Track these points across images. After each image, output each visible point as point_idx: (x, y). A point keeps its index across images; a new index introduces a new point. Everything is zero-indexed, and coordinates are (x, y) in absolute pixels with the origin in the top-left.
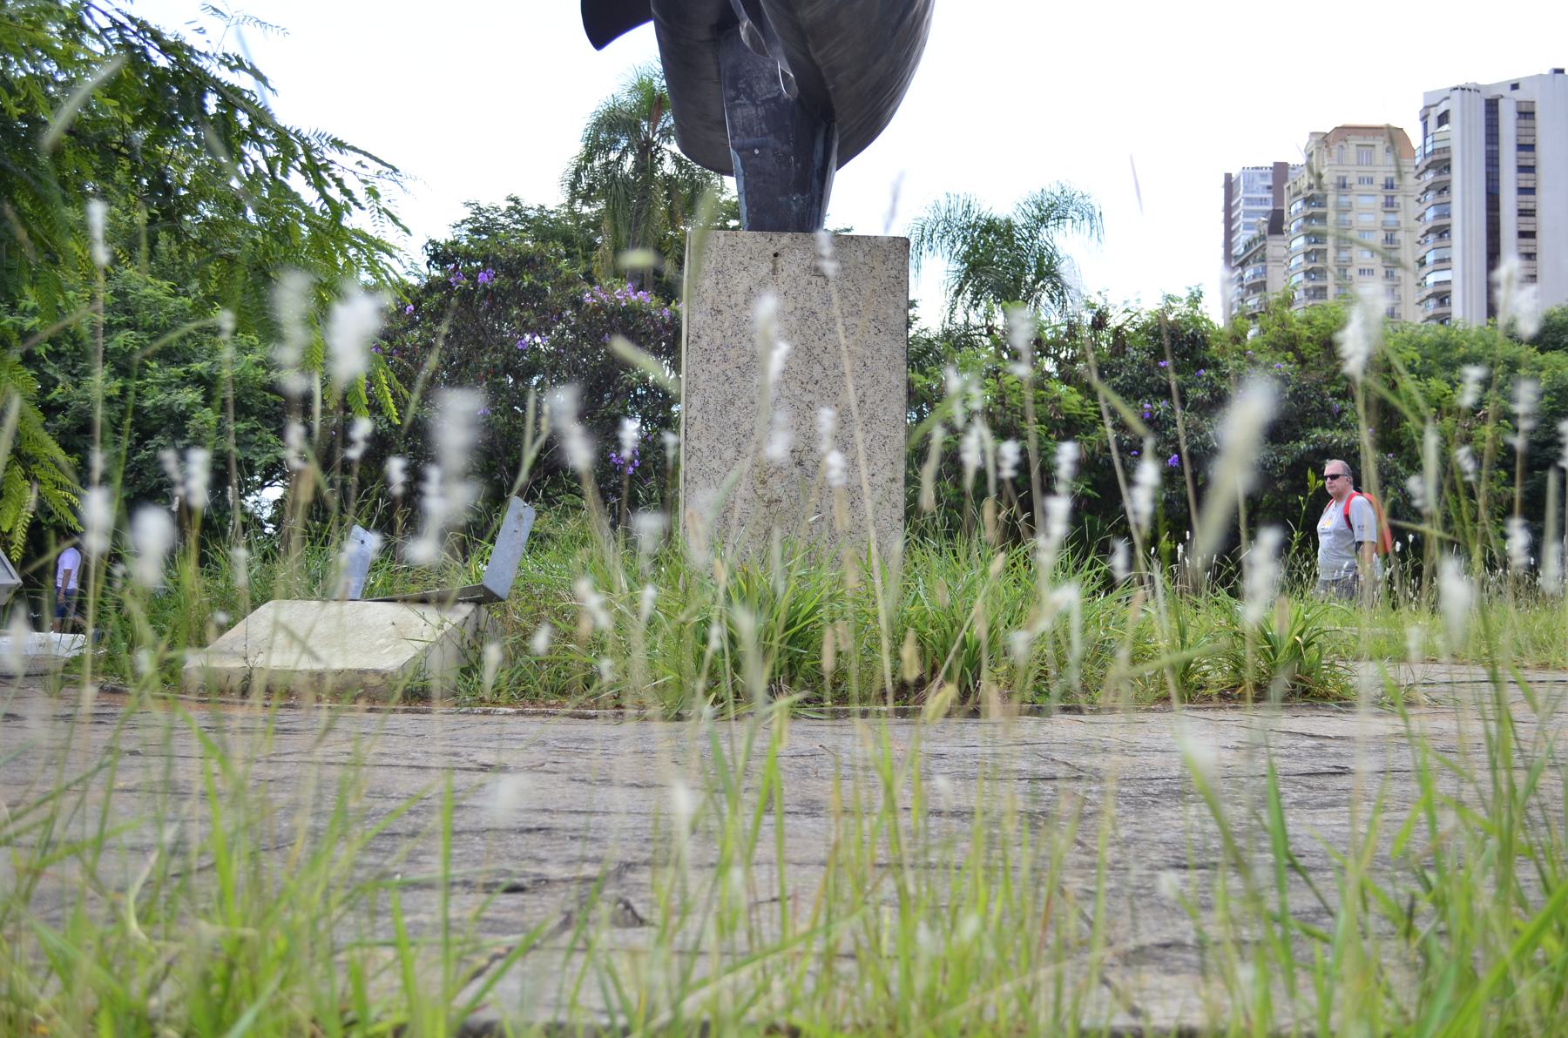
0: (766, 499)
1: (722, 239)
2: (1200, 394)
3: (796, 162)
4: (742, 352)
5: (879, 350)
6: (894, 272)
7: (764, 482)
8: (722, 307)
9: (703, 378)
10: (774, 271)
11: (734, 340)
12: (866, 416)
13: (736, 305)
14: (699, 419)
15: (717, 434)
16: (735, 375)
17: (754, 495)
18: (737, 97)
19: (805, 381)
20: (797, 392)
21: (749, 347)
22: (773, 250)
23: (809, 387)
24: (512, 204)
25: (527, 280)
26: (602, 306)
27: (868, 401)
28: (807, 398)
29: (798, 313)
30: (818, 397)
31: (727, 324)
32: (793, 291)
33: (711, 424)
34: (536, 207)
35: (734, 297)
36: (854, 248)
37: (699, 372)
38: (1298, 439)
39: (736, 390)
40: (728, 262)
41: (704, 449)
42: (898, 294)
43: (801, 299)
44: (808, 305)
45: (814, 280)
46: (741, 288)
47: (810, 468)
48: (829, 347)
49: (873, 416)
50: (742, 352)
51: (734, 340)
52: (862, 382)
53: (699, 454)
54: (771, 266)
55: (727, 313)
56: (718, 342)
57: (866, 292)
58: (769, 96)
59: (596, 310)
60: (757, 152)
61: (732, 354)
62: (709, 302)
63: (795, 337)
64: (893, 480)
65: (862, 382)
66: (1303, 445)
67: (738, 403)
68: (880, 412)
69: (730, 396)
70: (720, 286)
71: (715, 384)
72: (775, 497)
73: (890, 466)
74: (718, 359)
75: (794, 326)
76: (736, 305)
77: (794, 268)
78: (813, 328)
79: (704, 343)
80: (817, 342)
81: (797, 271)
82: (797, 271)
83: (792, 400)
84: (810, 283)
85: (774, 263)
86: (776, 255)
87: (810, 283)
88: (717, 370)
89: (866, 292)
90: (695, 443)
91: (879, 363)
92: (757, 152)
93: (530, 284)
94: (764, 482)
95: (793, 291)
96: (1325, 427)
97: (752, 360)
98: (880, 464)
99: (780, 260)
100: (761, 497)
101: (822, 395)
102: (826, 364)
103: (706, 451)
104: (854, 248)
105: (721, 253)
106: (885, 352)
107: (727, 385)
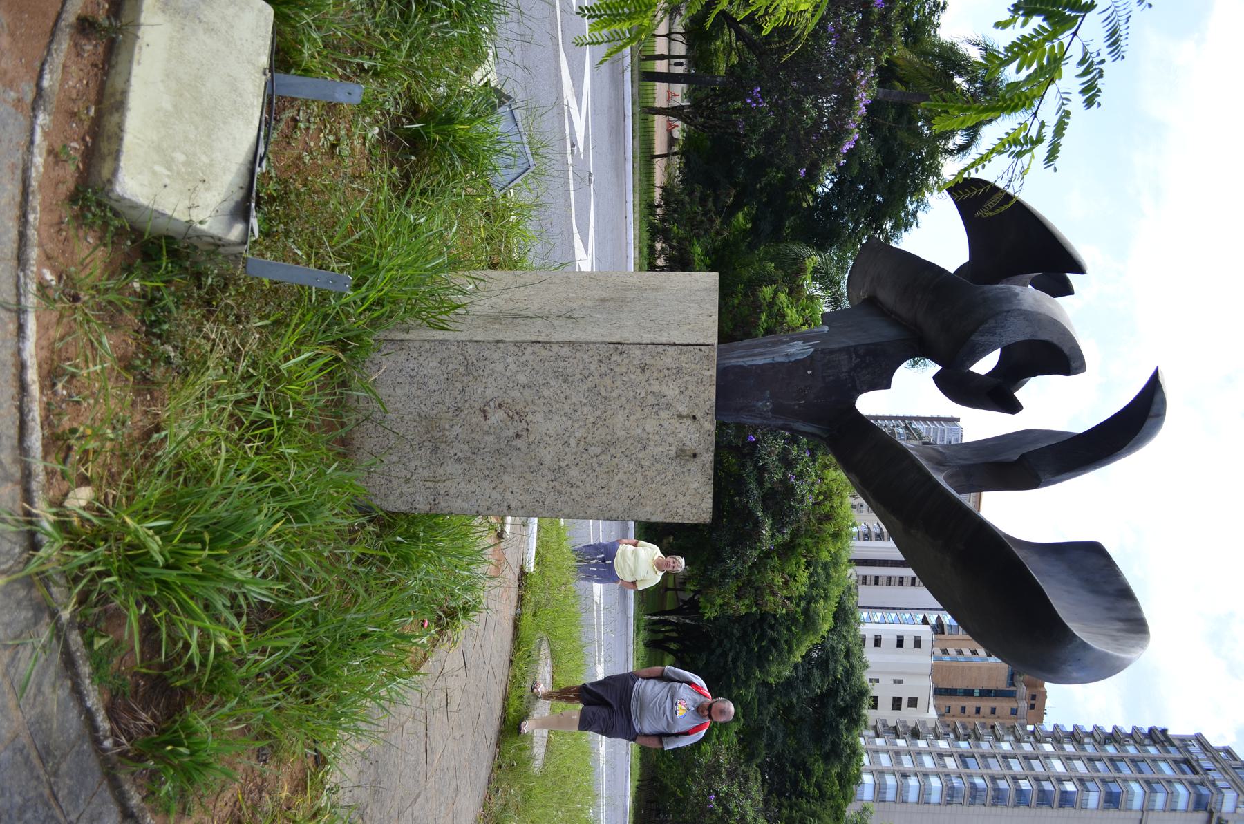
0: (486, 408)
1: (708, 373)
2: (794, 453)
3: (799, 404)
4: (609, 390)
5: (615, 499)
6: (681, 511)
7: (500, 406)
8: (648, 373)
9: (586, 357)
10: (680, 416)
11: (619, 383)
15: (538, 368)
16: (589, 383)
17: (488, 399)
18: (857, 356)
19: (587, 440)
20: (577, 434)
21: (614, 395)
22: (699, 415)
23: (582, 444)
24: (941, 5)
25: (876, 31)
26: (855, 84)
27: (572, 490)
28: (573, 442)
29: (645, 436)
30: (574, 450)
31: (633, 377)
32: (663, 432)
33: (546, 364)
34: (940, 21)
35: (657, 382)
36: (701, 480)
37: (591, 353)
38: (763, 511)
39: (577, 384)
40: (688, 378)
41: (524, 358)
42: (663, 514)
43: (657, 437)
44: (652, 443)
45: (673, 448)
46: (664, 389)
47: (514, 444)
49: (560, 493)
50: (609, 390)
51: (619, 383)
52: (588, 485)
53: (520, 354)
54: (685, 414)
55: (642, 377)
56: (616, 369)
57: (663, 490)
58: (858, 382)
59: (853, 80)
60: (809, 372)
61: (607, 381)
62: (652, 362)
63: (623, 433)
65: (588, 485)
66: (760, 514)
67: (565, 386)
68: (564, 498)
69: (571, 379)
70: (666, 371)
71: (581, 367)
72: (489, 415)
76: (650, 385)
77: (683, 432)
78: (632, 448)
79: (616, 357)
80: (620, 450)
84: (670, 445)
85: (687, 416)
86: (694, 417)
88: (592, 368)
89: (663, 490)
90: (529, 350)
92: (809, 372)
93: (873, 34)
94: (500, 406)
96: (772, 526)
98: (521, 498)
99: (690, 421)
100: (487, 404)
101: (576, 454)
102: (603, 457)
103: (523, 359)
104: (701, 480)
105: (695, 372)
106: (614, 504)
107: (580, 377)
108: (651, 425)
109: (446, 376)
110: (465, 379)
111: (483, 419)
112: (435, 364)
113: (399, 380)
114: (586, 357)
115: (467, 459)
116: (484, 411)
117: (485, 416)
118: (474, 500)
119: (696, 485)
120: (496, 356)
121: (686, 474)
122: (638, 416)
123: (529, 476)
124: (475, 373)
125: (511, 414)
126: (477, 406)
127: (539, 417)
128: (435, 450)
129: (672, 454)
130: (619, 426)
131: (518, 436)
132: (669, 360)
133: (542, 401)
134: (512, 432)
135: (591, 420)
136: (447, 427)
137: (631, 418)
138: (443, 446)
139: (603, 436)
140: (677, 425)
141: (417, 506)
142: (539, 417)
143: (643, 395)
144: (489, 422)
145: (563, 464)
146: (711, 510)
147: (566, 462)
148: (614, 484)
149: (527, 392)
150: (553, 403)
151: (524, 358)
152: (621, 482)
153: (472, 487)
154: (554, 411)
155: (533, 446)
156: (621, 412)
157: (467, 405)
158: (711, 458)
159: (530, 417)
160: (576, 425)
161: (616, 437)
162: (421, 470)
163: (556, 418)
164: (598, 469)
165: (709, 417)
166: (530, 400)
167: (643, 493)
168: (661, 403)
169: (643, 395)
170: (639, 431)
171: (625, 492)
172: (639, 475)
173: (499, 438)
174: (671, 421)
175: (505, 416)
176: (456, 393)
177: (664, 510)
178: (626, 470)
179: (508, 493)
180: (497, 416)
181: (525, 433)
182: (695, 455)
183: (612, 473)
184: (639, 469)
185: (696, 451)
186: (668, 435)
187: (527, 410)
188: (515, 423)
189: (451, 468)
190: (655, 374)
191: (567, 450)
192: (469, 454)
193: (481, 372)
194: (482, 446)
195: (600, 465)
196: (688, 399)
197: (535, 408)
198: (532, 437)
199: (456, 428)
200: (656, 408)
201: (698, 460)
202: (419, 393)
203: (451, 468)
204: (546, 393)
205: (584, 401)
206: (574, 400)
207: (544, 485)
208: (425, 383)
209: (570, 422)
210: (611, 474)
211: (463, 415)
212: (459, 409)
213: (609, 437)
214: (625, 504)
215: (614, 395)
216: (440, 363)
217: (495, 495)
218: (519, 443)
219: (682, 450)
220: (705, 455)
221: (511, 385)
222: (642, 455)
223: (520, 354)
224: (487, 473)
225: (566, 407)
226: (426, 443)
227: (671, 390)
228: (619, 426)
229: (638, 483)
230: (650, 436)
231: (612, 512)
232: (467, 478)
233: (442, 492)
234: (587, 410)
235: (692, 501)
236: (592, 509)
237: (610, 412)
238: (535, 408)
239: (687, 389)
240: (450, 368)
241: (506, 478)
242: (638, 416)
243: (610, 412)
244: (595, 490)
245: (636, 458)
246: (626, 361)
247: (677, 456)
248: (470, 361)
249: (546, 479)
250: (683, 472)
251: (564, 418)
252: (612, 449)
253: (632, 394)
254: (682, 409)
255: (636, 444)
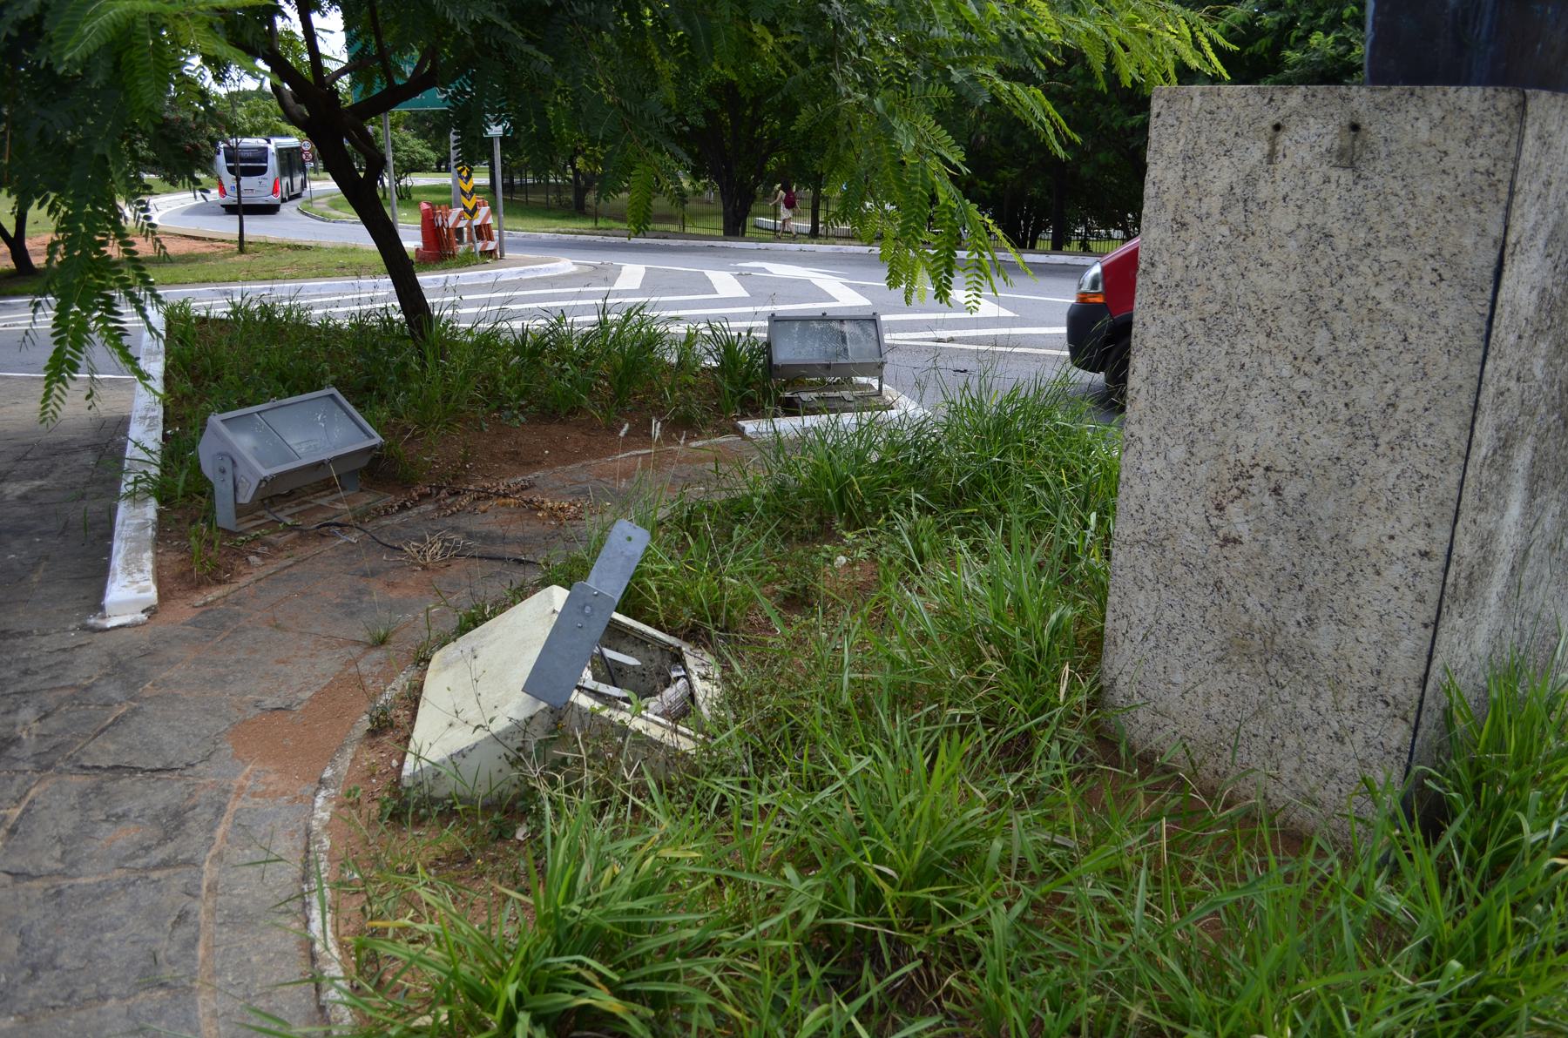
1: (1197, 101)
5: (1434, 314)
6: (1484, 163)
7: (1220, 508)
8: (1188, 218)
9: (1153, 330)
10: (1271, 157)
11: (1200, 274)
12: (1395, 433)
13: (1208, 215)
14: (1143, 392)
15: (1164, 421)
16: (1196, 330)
17: (1205, 524)
19: (1300, 355)
20: (1286, 373)
21: (1220, 287)
22: (1272, 117)
23: (1306, 367)
27: (1402, 407)
28: (1301, 384)
29: (1302, 234)
30: (1318, 385)
31: (1192, 247)
32: (1298, 194)
33: (1159, 404)
35: (1205, 200)
36: (1413, 113)
37: (1148, 320)
39: (1196, 356)
40: (1202, 141)
41: (1146, 440)
42: (1487, 206)
43: (1309, 208)
44: (1320, 220)
45: (1334, 174)
46: (1219, 186)
47: (1291, 503)
48: (1347, 299)
49: (1406, 435)
50: (1210, 294)
51: (1200, 274)
53: (1139, 446)
54: (1267, 148)
55: (1195, 228)
56: (1178, 276)
57: (1426, 202)
61: (1196, 296)
62: (1170, 207)
63: (1293, 277)
64: (1425, 555)
67: (1197, 377)
68: (1420, 429)
69: (1187, 365)
70: (1189, 182)
71: (1168, 342)
72: (1234, 534)
73: (1421, 530)
74: (1176, 302)
75: (1294, 257)
76: (1208, 215)
77: (1304, 151)
78: (1324, 263)
80: (1327, 289)
81: (1308, 158)
82: (1308, 158)
83: (1276, 385)
84: (1327, 180)
85: (1273, 142)
86: (1277, 127)
87: (1327, 180)
88: (1172, 321)
89: (1426, 202)
91: (1432, 339)
94: (1220, 508)
95: (1298, 194)
97: (1223, 308)
98: (1407, 521)
99: (1283, 137)
101: (1325, 383)
102: (1338, 328)
106: (1446, 320)
107: (1184, 345)
108: (1283, 219)
109: (1160, 586)
110: (1169, 555)
111: (1239, 548)
112: (1141, 596)
113: (1160, 669)
114: (1153, 330)
115: (1309, 603)
116: (1226, 540)
117: (1235, 541)
118: (1397, 624)
119: (1423, 125)
120: (1139, 490)
121: (1394, 147)
122: (1262, 244)
123: (1361, 491)
124: (1163, 534)
125: (1235, 492)
126: (1215, 550)
127: (1247, 439)
128: (1286, 659)
129: (1346, 177)
130: (1277, 284)
131: (1277, 491)
132: (1170, 175)
133: (1218, 426)
134: (1270, 502)
135: (1262, 338)
136: (1246, 619)
137: (1266, 257)
138: (1278, 639)
139: (1296, 321)
140: (1287, 163)
141: (1395, 743)
142: (1247, 439)
143: (1224, 230)
144: (1246, 538)
145: (1344, 414)
146: (1490, 91)
147: (1340, 406)
148: (1399, 312)
149: (1203, 451)
150: (1224, 407)
151: (1146, 440)
152: (1397, 296)
153: (1369, 616)
154: (1237, 409)
155: (1300, 466)
156: (1253, 276)
157: (1212, 568)
158: (1364, 91)
159: (1245, 457)
160: (1269, 371)
161: (1298, 294)
162: (1320, 703)
163: (1251, 407)
164: (1362, 342)
165: (1278, 95)
166: (1214, 450)
167: (1429, 250)
168: (1243, 197)
169: (1224, 230)
170: (1292, 244)
171: (1422, 290)
172: (1387, 255)
173: (1277, 529)
174: (1278, 178)
175: (1238, 503)
176: (1190, 581)
177: (1477, 204)
178: (1370, 281)
179: (1392, 546)
180: (1237, 520)
181: (1273, 476)
182: (1355, 127)
183: (1375, 313)
184: (1373, 252)
185: (1345, 122)
186: (1307, 183)
187: (1231, 459)
188: (1254, 489)
189: (1324, 640)
190: (1191, 203)
191: (1315, 399)
192: (1301, 597)
193: (1161, 524)
194: (1288, 566)
195: (1354, 336)
196: (1240, 141)
197: (1229, 442)
198: (1282, 464)
199: (1249, 605)
200: (1252, 206)
201: (1364, 121)
202: (1184, 645)
203: (1324, 640)
204: (1205, 416)
205: (1226, 346)
206: (1222, 366)
207: (1383, 464)
208: (1170, 628)
209: (1262, 382)
210: (1376, 316)
211: (1228, 582)
212: (1218, 584)
213: (1299, 308)
214: (1450, 293)
215: (1220, 287)
216: (1141, 588)
217: (1394, 573)
218: (1291, 490)
219: (1341, 154)
220: (1355, 104)
221: (1186, 475)
222: (1342, 244)
223: (1139, 446)
224: (1342, 576)
225: (1234, 383)
226: (1272, 671)
227: (1222, 175)
228: (1277, 284)
229: (1404, 258)
230: (1304, 222)
231: (1466, 327)
232: (1348, 618)
233: (1371, 681)
234: (1242, 346)
235: (1462, 136)
236: (1453, 371)
237: (1251, 299)
238: (1229, 442)
239: (1222, 142)
240: (1151, 576)
241: (1358, 541)
242: (1262, 244)
243: (1251, 299)
244: (1407, 357)
245: (1348, 257)
246: (1166, 256)
247: (1352, 166)
248: (1143, 536)
249: (1371, 457)
250: (1389, 155)
251: (1254, 393)
252: (1324, 306)
253: (1221, 252)
254: (1259, 150)
255: (1317, 253)
